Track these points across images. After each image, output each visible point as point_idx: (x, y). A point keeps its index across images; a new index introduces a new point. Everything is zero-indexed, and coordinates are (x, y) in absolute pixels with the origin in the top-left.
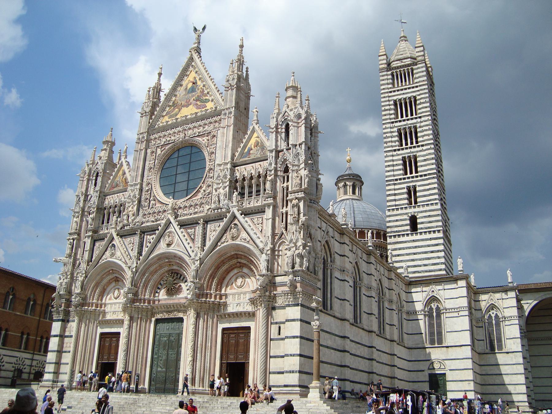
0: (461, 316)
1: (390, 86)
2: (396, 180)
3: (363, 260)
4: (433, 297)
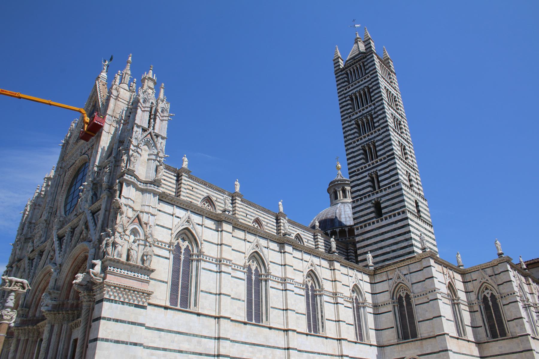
0: (431, 300)
1: (346, 83)
2: (358, 170)
3: (270, 249)
4: (401, 284)
